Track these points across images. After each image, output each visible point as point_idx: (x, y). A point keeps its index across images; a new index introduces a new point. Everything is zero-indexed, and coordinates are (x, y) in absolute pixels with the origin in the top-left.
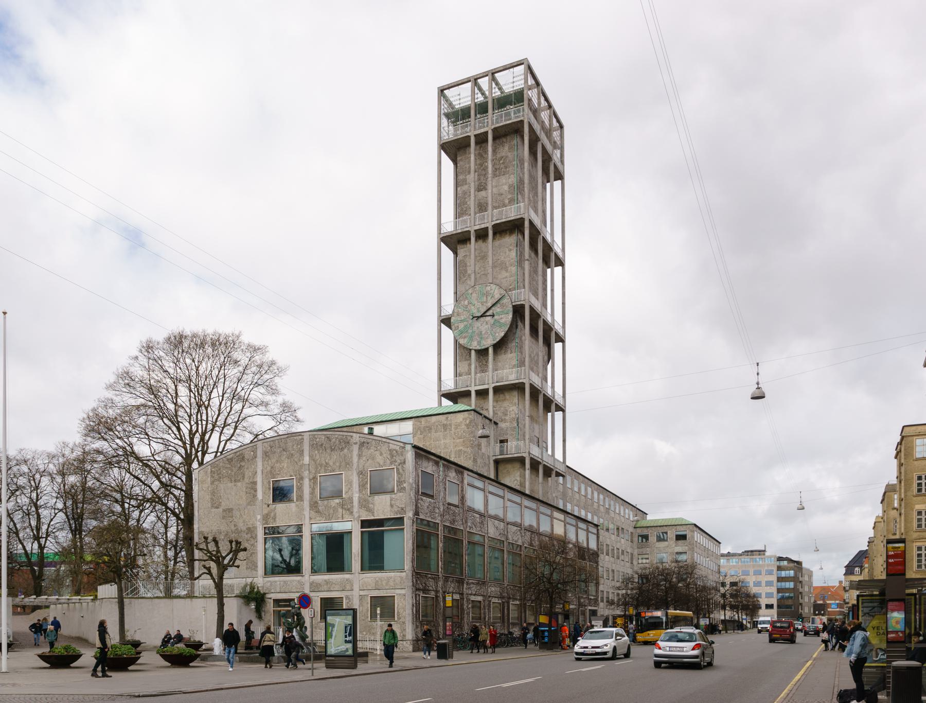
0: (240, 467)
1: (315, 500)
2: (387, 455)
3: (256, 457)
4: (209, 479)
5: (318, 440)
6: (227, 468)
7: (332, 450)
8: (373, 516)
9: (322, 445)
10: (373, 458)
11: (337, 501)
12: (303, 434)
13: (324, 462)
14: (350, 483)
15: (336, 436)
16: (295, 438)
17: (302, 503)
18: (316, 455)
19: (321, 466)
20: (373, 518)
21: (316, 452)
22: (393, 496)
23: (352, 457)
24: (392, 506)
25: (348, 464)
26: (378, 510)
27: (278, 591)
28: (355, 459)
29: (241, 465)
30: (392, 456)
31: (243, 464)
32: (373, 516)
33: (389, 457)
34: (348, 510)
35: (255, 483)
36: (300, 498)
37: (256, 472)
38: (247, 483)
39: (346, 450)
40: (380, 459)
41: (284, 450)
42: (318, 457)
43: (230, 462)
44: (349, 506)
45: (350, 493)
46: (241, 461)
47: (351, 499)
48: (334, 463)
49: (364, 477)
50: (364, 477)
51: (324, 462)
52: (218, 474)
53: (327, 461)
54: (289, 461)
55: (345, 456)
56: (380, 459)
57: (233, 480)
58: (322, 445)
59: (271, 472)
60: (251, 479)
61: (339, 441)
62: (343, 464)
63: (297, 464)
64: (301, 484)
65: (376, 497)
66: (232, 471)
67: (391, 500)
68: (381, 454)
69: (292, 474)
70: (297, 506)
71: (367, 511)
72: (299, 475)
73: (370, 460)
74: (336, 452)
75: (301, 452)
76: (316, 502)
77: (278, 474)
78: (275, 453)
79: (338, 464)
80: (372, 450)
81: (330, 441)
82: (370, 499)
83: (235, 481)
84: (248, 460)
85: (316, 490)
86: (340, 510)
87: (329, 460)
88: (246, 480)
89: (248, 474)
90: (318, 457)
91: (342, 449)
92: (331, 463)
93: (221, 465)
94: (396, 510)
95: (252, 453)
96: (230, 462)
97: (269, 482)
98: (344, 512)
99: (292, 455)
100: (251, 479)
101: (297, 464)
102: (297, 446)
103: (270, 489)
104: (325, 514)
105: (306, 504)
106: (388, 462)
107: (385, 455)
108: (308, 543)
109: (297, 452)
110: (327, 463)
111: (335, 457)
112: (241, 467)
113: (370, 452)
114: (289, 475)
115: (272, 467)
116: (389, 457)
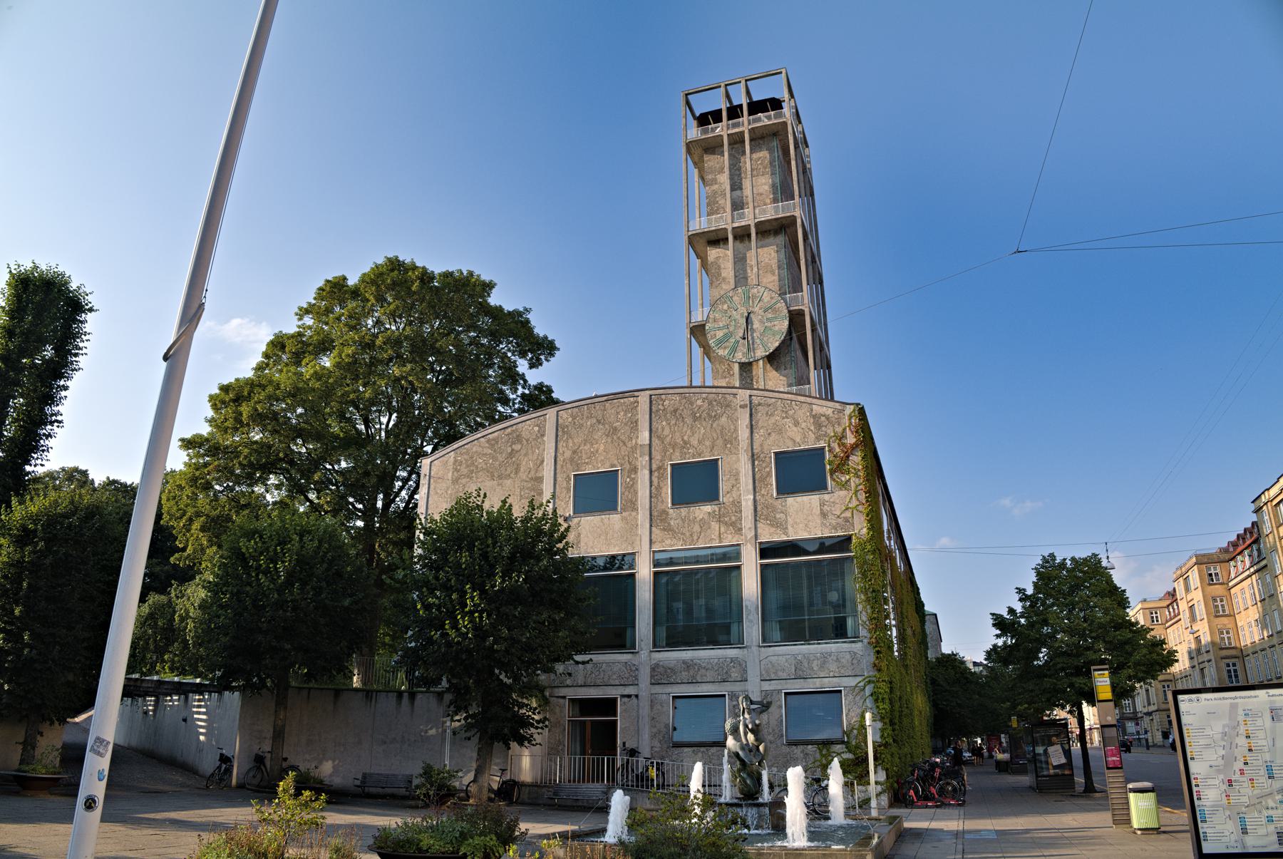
0: (511, 454)
1: (661, 507)
2: (808, 424)
3: (543, 435)
4: (450, 474)
5: (667, 403)
6: (486, 454)
7: (695, 419)
8: (786, 534)
9: (675, 411)
10: (780, 432)
11: (708, 508)
12: (636, 394)
13: (679, 441)
14: (736, 476)
15: (704, 395)
16: (622, 401)
17: (634, 514)
18: (663, 429)
19: (674, 446)
20: (785, 538)
21: (664, 423)
22: (826, 497)
23: (736, 430)
24: (824, 515)
25: (729, 441)
26: (796, 523)
27: (580, 682)
28: (744, 433)
29: (513, 450)
30: (819, 426)
31: (517, 447)
32: (786, 534)
33: (812, 428)
34: (733, 524)
35: (540, 480)
36: (632, 505)
37: (543, 461)
38: (522, 481)
39: (724, 419)
40: (794, 433)
41: (599, 422)
42: (667, 431)
43: (493, 445)
44: (733, 518)
45: (735, 494)
46: (513, 443)
47: (737, 505)
48: (700, 442)
49: (764, 465)
50: (764, 465)
51: (679, 441)
52: (468, 466)
53: (686, 438)
54: (609, 440)
55: (723, 428)
56: (794, 433)
57: (496, 474)
58: (675, 411)
59: (572, 460)
60: (533, 472)
61: (710, 403)
62: (720, 442)
63: (624, 444)
64: (634, 479)
65: (790, 500)
66: (495, 459)
67: (822, 504)
68: (796, 424)
69: (616, 462)
70: (623, 519)
71: (772, 525)
72: (630, 463)
73: (773, 434)
74: (704, 423)
75: (634, 425)
76: (664, 512)
77: (587, 463)
78: (581, 426)
79: (708, 443)
80: (778, 418)
81: (692, 404)
82: (778, 503)
83: (500, 477)
84: (527, 440)
85: (664, 490)
86: (715, 525)
87: (689, 436)
88: (523, 475)
89: (526, 463)
90: (667, 431)
91: (716, 418)
92: (695, 443)
93: (474, 449)
94: (834, 522)
95: (536, 429)
96: (493, 445)
97: (568, 477)
98: (722, 529)
99: (615, 429)
100: (533, 472)
101: (624, 444)
102: (625, 415)
103: (569, 490)
104: (683, 534)
105: (642, 517)
106: (812, 436)
107: (804, 425)
108: (647, 588)
109: (626, 424)
110: (685, 443)
111: (703, 431)
112: (512, 454)
113: (772, 420)
114: (608, 464)
115: (574, 452)
116: (812, 428)
